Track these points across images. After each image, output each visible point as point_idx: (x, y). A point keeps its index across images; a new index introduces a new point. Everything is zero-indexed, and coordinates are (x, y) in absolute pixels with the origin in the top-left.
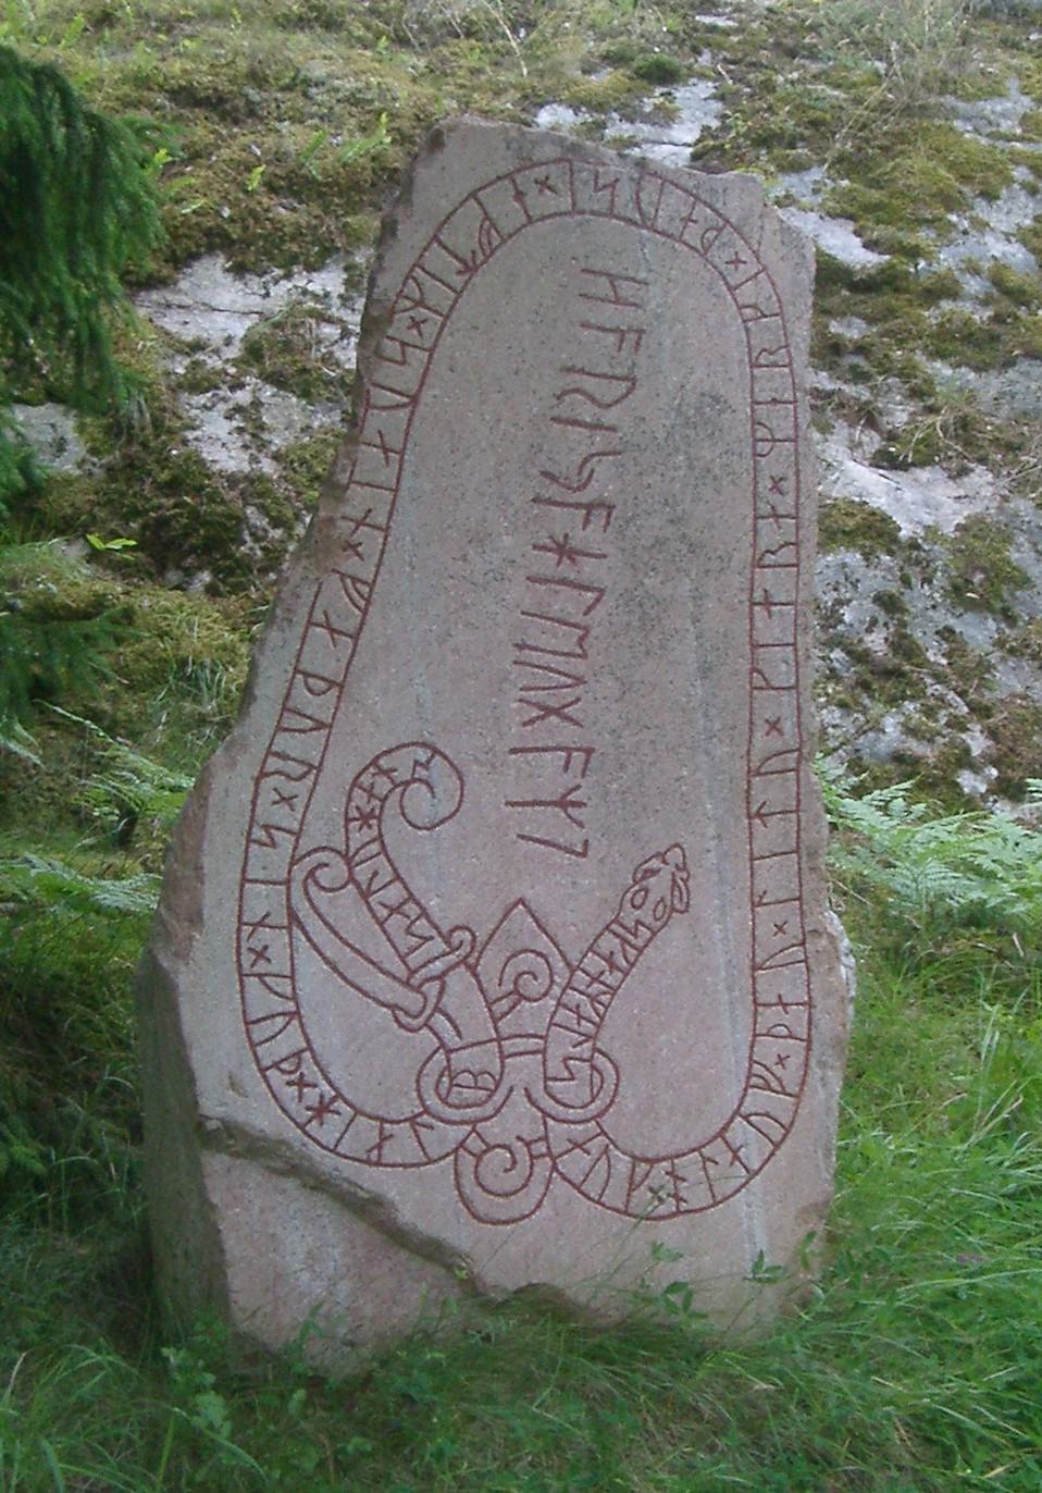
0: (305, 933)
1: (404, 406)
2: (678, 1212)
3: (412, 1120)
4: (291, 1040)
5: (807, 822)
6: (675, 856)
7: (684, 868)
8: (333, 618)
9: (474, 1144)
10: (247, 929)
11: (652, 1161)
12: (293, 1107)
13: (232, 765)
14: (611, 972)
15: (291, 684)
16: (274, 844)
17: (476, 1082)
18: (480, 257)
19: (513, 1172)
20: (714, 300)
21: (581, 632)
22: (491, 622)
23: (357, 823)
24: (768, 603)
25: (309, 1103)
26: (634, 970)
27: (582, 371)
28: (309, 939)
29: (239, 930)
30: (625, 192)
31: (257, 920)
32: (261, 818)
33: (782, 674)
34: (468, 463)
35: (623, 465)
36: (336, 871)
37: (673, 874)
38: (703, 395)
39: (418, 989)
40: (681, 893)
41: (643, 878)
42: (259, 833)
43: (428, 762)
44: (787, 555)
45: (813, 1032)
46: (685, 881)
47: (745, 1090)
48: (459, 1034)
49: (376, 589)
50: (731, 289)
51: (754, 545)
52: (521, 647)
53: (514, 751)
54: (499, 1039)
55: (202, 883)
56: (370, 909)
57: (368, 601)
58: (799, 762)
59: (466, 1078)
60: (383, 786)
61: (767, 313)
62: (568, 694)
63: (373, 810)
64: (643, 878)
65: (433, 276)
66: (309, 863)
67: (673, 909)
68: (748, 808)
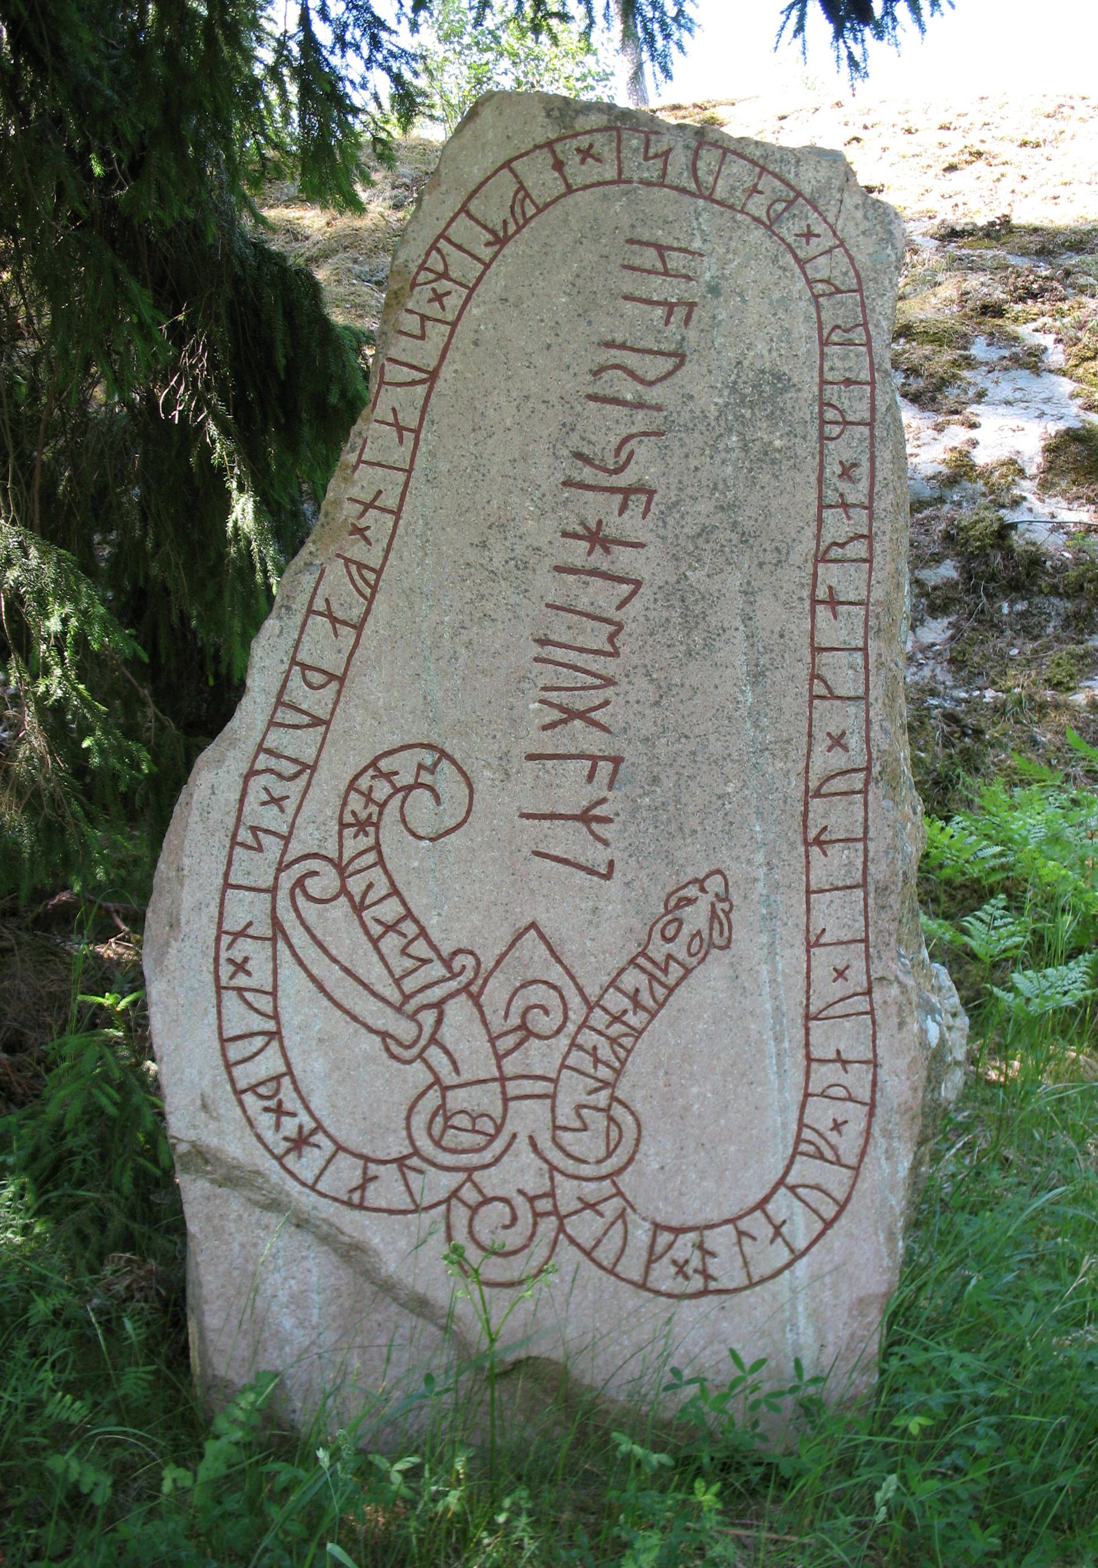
0: (291, 947)
1: (422, 382)
2: (704, 1292)
3: (400, 1162)
4: (269, 1063)
5: (877, 851)
6: (715, 884)
7: (726, 899)
8: (335, 607)
9: (469, 1194)
10: (226, 940)
11: (678, 1231)
12: (269, 1136)
13: (220, 762)
14: (635, 1013)
15: (287, 677)
16: (260, 849)
17: (474, 1125)
18: (512, 228)
19: (513, 1229)
20: (780, 272)
21: (613, 628)
22: (510, 615)
23: (354, 830)
24: (833, 602)
25: (287, 1134)
26: (663, 1011)
27: (623, 346)
28: (295, 954)
29: (218, 940)
30: (680, 159)
31: (239, 928)
32: (249, 820)
33: (847, 682)
34: (490, 442)
35: (666, 447)
36: (325, 882)
37: (713, 905)
38: (763, 372)
39: (412, 1017)
40: (721, 924)
41: (677, 906)
42: (244, 835)
43: (435, 764)
44: (858, 549)
45: (878, 1096)
46: (727, 914)
47: (793, 1157)
48: (457, 1070)
49: (384, 576)
50: (801, 263)
51: (818, 537)
52: (543, 642)
53: (530, 757)
54: (502, 1079)
55: (182, 885)
56: (363, 925)
57: (374, 589)
58: (867, 783)
59: (462, 1121)
60: (382, 789)
61: (843, 288)
62: (596, 697)
63: (370, 816)
64: (677, 906)
65: (459, 247)
66: (298, 870)
67: (712, 945)
68: (805, 833)
